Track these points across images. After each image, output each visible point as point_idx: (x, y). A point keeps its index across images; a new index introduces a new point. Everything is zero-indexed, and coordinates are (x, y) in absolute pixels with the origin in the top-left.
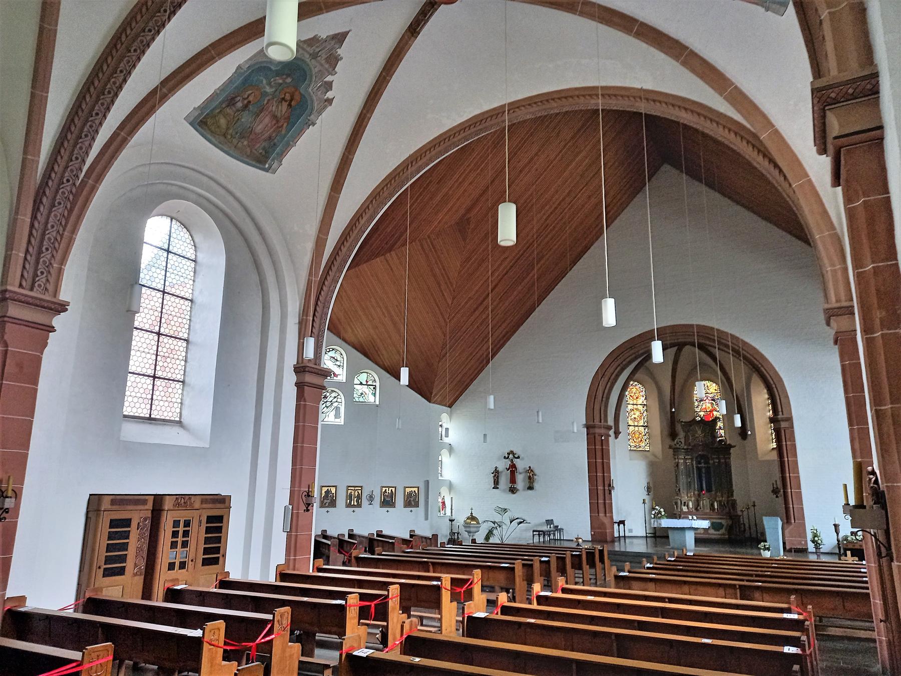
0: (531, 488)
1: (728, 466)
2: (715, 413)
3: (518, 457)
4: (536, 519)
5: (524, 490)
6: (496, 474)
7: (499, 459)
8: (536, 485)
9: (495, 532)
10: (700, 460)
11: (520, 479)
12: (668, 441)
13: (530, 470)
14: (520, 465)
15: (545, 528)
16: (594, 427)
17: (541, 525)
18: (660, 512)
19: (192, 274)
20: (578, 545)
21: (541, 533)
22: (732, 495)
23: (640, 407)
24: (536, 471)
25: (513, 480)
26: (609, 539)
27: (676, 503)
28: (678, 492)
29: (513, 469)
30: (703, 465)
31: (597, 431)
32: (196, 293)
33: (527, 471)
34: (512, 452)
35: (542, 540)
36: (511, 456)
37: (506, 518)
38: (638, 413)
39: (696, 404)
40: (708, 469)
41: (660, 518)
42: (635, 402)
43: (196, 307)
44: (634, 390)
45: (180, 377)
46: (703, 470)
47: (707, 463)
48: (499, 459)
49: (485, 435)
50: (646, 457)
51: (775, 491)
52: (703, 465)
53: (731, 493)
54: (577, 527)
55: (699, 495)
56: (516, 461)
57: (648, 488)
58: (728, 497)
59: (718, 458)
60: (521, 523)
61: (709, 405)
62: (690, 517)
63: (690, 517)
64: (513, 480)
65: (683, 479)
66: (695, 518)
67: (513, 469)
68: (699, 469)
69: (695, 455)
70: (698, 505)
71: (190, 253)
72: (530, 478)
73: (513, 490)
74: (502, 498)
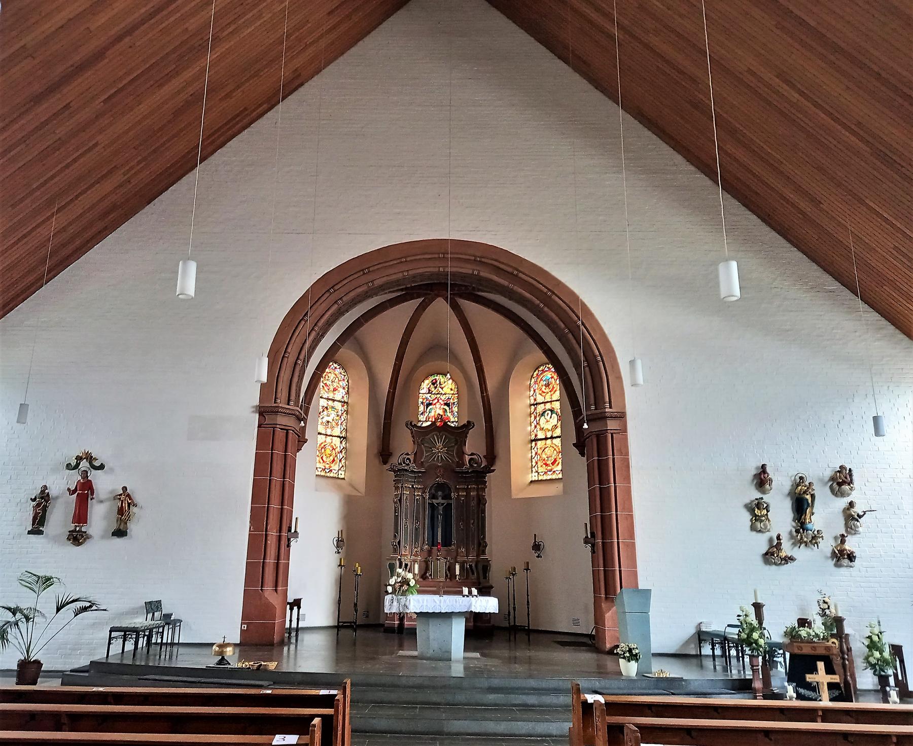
0: (120, 533)
1: (481, 502)
3: (102, 467)
4: (122, 602)
5: (103, 537)
6: (43, 501)
8: (133, 528)
9: (12, 633)
10: (442, 492)
11: (100, 515)
12: (376, 462)
14: (103, 484)
15: (140, 621)
16: (275, 411)
17: (134, 612)
18: (406, 582)
20: (222, 661)
21: (126, 632)
22: (484, 553)
23: (338, 405)
24: (137, 498)
25: (81, 516)
26: (276, 638)
27: (392, 568)
28: (396, 549)
29: (84, 492)
30: (440, 500)
31: (282, 420)
33: (117, 497)
34: (89, 458)
35: (130, 646)
36: (84, 464)
37: (47, 600)
38: (333, 415)
39: (421, 408)
40: (448, 508)
41: (404, 594)
42: (331, 396)
44: (332, 376)
46: (441, 508)
47: (447, 497)
49: (23, 407)
50: (340, 488)
51: (586, 541)
52: (440, 500)
53: (482, 546)
54: (213, 621)
55: (430, 553)
56: (94, 476)
57: (338, 541)
58: (478, 556)
59: (467, 490)
60: (85, 609)
62: (466, 591)
63: (466, 591)
65: (407, 525)
66: (475, 591)
67: (84, 492)
68: (432, 506)
69: (430, 483)
70: (427, 569)
72: (121, 511)
73: (77, 538)
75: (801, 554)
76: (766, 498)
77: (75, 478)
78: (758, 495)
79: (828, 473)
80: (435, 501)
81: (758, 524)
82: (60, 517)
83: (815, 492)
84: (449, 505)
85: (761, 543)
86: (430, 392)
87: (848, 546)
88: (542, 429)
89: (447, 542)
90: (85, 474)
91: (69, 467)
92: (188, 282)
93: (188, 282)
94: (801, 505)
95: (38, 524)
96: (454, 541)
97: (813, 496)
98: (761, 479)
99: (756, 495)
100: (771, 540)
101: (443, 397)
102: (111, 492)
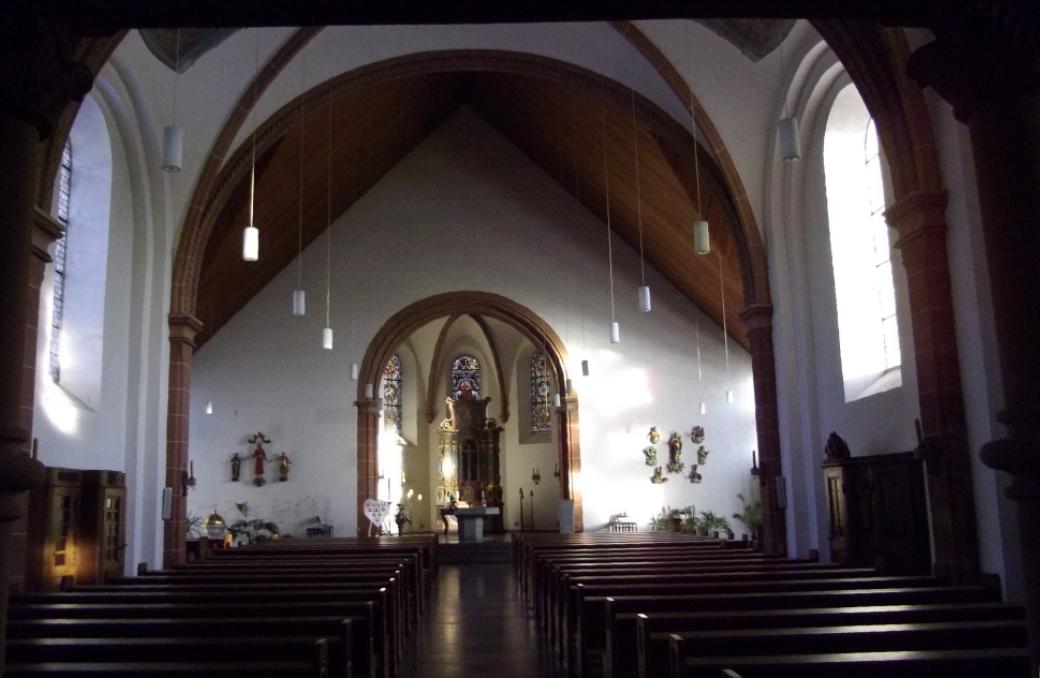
0: (283, 479)
2: (473, 392)
3: (268, 442)
6: (236, 461)
7: (241, 443)
8: (290, 475)
11: (269, 469)
14: (272, 451)
25: (259, 470)
29: (259, 456)
34: (261, 436)
36: (259, 440)
46: (469, 456)
48: (241, 443)
49: (236, 412)
52: (469, 451)
54: (345, 527)
56: (265, 447)
64: (259, 470)
67: (259, 456)
73: (259, 482)
74: (243, 491)
75: (672, 477)
77: (255, 447)
78: (651, 444)
80: (467, 451)
81: (651, 462)
82: (248, 470)
83: (683, 442)
84: (475, 454)
86: (460, 368)
88: (540, 396)
89: (474, 477)
90: (259, 446)
91: (250, 442)
96: (478, 476)
97: (680, 444)
101: (470, 372)
102: (276, 455)
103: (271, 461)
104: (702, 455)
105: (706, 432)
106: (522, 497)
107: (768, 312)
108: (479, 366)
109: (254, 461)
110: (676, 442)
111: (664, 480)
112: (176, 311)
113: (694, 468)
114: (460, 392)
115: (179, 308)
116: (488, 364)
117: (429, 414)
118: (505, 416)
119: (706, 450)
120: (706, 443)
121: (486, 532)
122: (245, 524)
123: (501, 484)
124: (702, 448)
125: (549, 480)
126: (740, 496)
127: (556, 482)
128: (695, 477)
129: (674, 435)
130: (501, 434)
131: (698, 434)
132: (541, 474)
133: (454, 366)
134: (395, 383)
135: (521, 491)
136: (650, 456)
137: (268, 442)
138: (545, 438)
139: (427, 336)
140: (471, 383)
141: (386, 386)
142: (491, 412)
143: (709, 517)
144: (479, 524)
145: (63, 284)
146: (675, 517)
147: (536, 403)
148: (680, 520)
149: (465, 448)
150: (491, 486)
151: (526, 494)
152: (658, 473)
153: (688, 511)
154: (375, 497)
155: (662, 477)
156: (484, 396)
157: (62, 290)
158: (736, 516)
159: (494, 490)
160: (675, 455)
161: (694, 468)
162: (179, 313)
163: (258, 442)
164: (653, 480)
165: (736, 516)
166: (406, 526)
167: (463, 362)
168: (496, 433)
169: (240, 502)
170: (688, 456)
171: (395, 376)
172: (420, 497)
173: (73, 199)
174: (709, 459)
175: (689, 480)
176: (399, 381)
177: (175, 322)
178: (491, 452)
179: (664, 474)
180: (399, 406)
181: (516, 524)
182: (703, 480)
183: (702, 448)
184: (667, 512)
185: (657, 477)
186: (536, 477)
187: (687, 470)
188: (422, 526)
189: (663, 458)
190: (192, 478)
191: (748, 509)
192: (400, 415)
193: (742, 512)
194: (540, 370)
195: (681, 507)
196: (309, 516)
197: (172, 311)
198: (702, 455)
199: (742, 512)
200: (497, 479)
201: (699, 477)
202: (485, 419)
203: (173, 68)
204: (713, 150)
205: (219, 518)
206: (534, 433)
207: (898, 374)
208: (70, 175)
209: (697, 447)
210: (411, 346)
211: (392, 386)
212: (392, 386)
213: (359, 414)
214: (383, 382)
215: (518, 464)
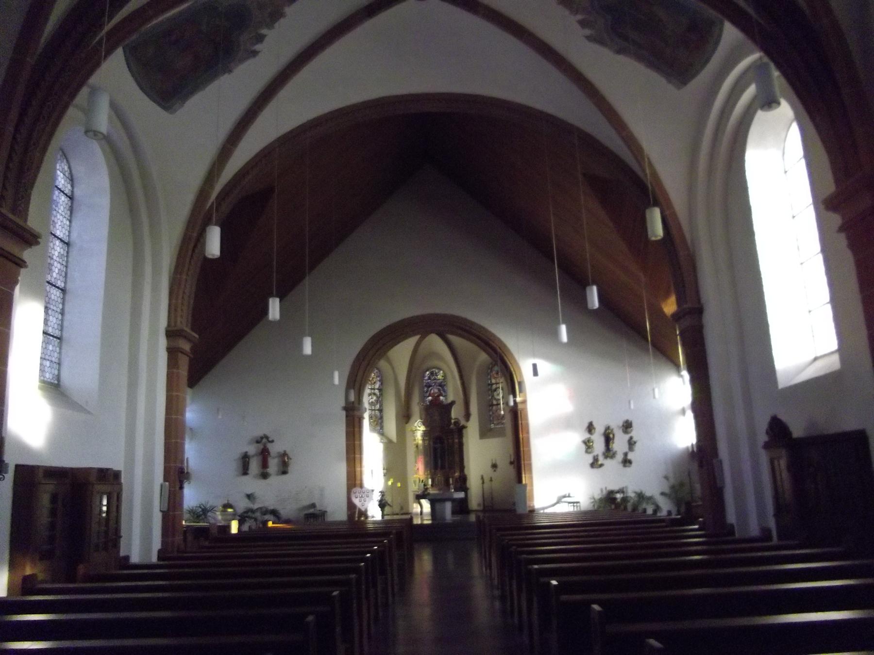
0: (284, 472)
2: (441, 398)
3: (272, 441)
5: (277, 475)
6: (245, 459)
7: (250, 443)
8: (290, 469)
11: (273, 464)
13: (285, 454)
14: (275, 449)
19: (69, 212)
24: (291, 455)
25: (265, 464)
32: (74, 235)
34: (267, 437)
43: (74, 252)
45: (57, 333)
48: (250, 443)
52: (439, 445)
61: (436, 391)
67: (264, 454)
71: (68, 189)
73: (265, 476)
74: (251, 484)
75: (608, 463)
76: (593, 437)
77: (261, 446)
79: (621, 424)
82: (254, 466)
85: (589, 459)
87: (630, 457)
91: (258, 442)
92: (307, 348)
93: (307, 348)
94: (608, 438)
95: (245, 471)
98: (590, 428)
99: (587, 436)
100: (594, 457)
102: (279, 453)
103: (274, 458)
104: (631, 444)
105: (634, 425)
106: (483, 483)
107: (699, 311)
108: (445, 376)
109: (260, 458)
110: (609, 434)
111: (601, 465)
112: (173, 324)
113: (626, 454)
114: (430, 398)
115: (176, 322)
116: (454, 378)
117: (405, 417)
118: (468, 416)
119: (634, 439)
120: (635, 433)
121: (454, 513)
122: (252, 511)
123: (466, 472)
124: (631, 438)
125: (506, 469)
126: (666, 478)
127: (511, 470)
128: (626, 462)
129: (608, 428)
130: (464, 431)
131: (627, 426)
132: (498, 463)
133: (424, 377)
134: (377, 391)
135: (482, 478)
136: (588, 445)
137: (272, 441)
138: (500, 433)
139: (402, 353)
140: (439, 390)
141: (370, 395)
142: (456, 413)
143: (641, 496)
144: (448, 506)
145: (64, 299)
146: (611, 496)
147: (492, 405)
148: (615, 499)
149: (435, 443)
150: (457, 474)
151: (487, 480)
152: (596, 459)
153: (621, 491)
154: (361, 486)
155: (600, 463)
156: (451, 399)
157: (63, 304)
158: (663, 494)
159: (460, 477)
160: (607, 443)
161: (626, 454)
162: (175, 326)
163: (263, 444)
164: (593, 465)
165: (663, 494)
166: (387, 509)
167: (432, 373)
168: (460, 430)
169: (249, 493)
170: (620, 444)
171: (377, 386)
172: (399, 485)
173: (73, 224)
174: (637, 447)
175: (621, 466)
176: (380, 390)
177: (171, 334)
178: (456, 446)
179: (601, 460)
180: (381, 410)
181: (479, 505)
182: (634, 464)
183: (631, 438)
184: (605, 492)
185: (595, 464)
186: (494, 466)
187: (620, 457)
188: (402, 508)
189: (599, 446)
190: (188, 473)
191: (673, 487)
192: (381, 418)
193: (667, 490)
194: (495, 378)
195: (615, 487)
196: (307, 503)
197: (169, 325)
198: (631, 444)
199: (667, 490)
200: (462, 468)
201: (630, 462)
202: (451, 419)
203: (165, 108)
204: (644, 171)
205: (231, 506)
206: (491, 430)
207: (836, 358)
208: (72, 203)
209: (627, 437)
210: (390, 362)
211: (375, 394)
212: (375, 394)
213: (347, 416)
214: (367, 391)
215: (479, 456)
